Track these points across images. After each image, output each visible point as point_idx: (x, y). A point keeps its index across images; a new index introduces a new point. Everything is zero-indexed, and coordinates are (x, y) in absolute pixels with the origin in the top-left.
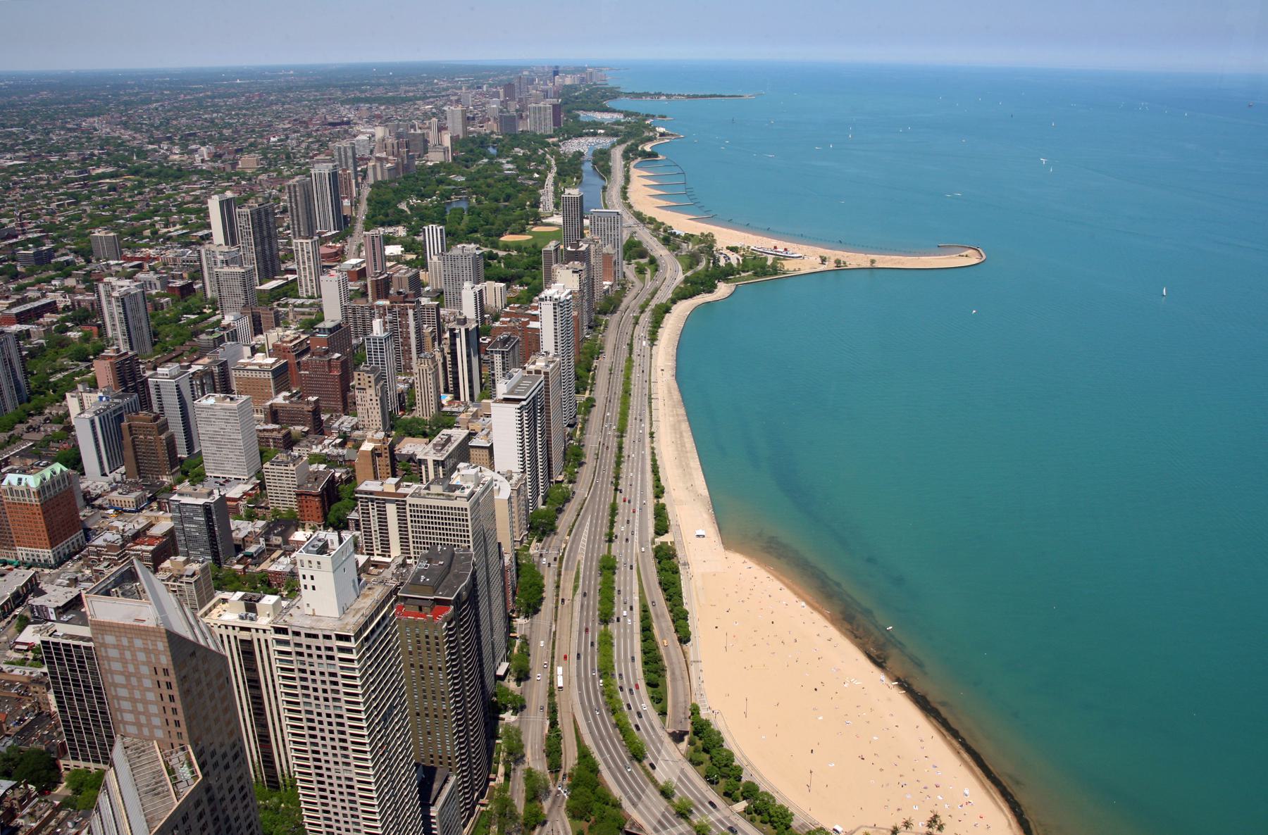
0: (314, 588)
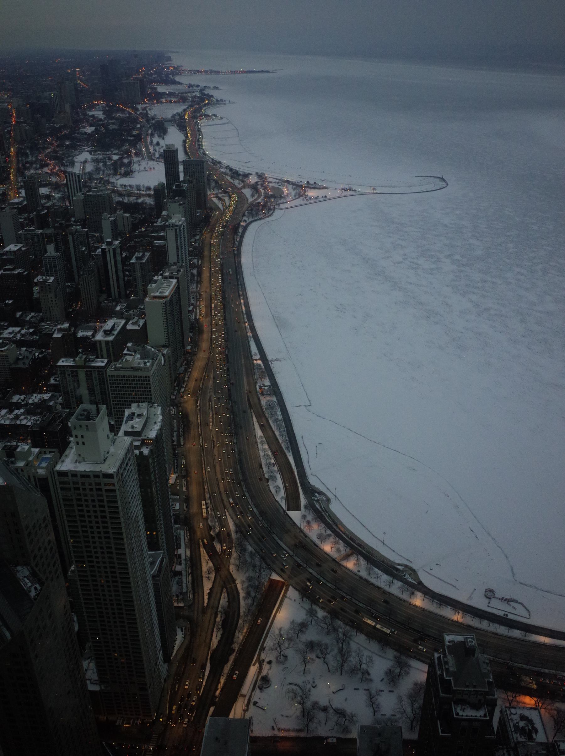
0: (83, 443)
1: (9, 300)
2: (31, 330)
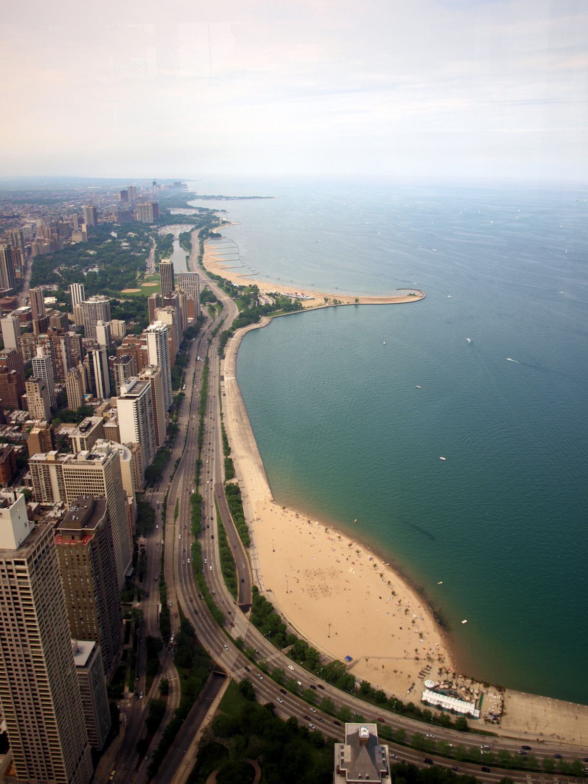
2: (16, 428)
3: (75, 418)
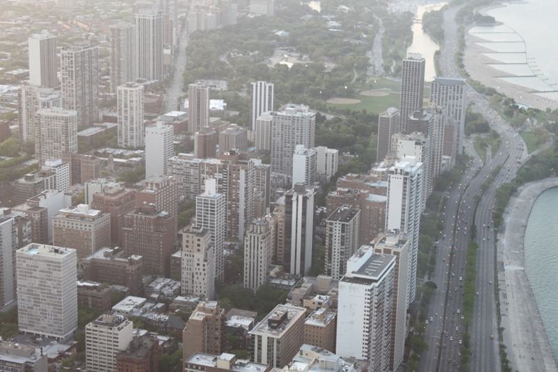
1: (136, 254)
2: (160, 305)
3: (262, 302)
